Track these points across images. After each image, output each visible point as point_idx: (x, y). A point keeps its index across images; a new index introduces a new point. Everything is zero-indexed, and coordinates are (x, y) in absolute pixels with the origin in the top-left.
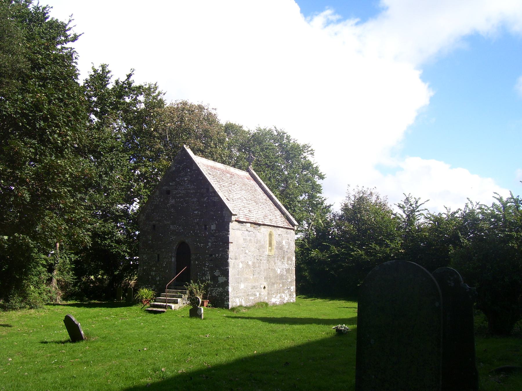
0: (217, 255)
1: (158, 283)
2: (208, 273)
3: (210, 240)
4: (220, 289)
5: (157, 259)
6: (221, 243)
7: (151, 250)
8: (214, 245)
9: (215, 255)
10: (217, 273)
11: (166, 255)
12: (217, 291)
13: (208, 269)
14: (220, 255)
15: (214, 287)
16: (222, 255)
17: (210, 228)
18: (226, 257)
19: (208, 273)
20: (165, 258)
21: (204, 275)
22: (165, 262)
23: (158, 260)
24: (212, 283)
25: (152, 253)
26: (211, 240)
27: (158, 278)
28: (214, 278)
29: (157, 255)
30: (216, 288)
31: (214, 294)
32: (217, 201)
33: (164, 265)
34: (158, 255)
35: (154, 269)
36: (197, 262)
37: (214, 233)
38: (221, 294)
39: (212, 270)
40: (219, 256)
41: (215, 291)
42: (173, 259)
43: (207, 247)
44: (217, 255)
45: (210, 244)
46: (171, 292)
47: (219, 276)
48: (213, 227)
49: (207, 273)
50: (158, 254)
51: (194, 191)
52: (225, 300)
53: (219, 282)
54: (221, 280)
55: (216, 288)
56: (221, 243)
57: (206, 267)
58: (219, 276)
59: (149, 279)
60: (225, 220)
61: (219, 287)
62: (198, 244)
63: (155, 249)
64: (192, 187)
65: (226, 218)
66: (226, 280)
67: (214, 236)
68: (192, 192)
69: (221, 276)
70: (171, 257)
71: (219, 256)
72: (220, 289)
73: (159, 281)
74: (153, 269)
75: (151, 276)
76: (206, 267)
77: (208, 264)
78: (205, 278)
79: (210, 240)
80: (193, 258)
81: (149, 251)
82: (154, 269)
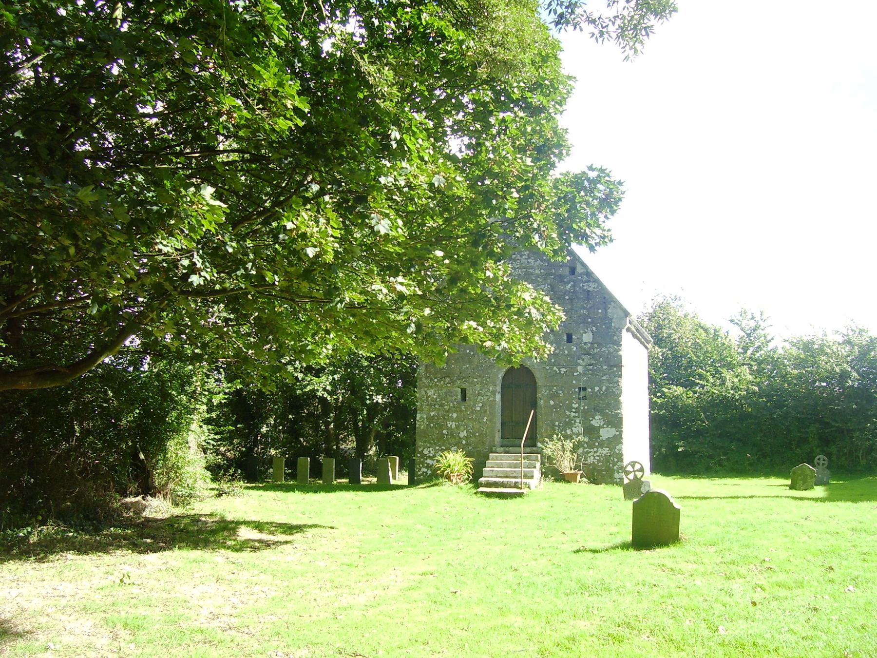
0: (597, 389)
1: (464, 442)
2: (578, 421)
3: (580, 361)
4: (605, 451)
5: (459, 396)
6: (605, 367)
7: (447, 380)
8: (590, 370)
9: (593, 389)
10: (596, 422)
11: (481, 390)
12: (598, 454)
13: (577, 415)
14: (604, 388)
15: (591, 446)
16: (608, 388)
17: (580, 339)
18: (617, 392)
19: (578, 421)
20: (479, 394)
21: (569, 424)
22: (479, 402)
23: (464, 398)
24: (586, 440)
25: (449, 385)
26: (583, 361)
27: (463, 434)
28: (591, 431)
29: (460, 390)
30: (595, 449)
31: (590, 460)
32: (595, 290)
33: (478, 409)
34: (463, 391)
35: (455, 415)
36: (552, 403)
37: (590, 348)
38: (607, 459)
39: (586, 416)
40: (601, 390)
41: (592, 454)
42: (498, 397)
43: (575, 374)
44: (597, 389)
45: (580, 369)
46: (499, 458)
47: (601, 427)
48: (587, 337)
49: (575, 422)
50: (462, 389)
51: (542, 271)
52: (614, 470)
53: (601, 438)
54: (606, 433)
55: (595, 449)
56: (605, 367)
57: (574, 410)
58: (601, 427)
59: (444, 434)
60: (613, 325)
61: (601, 445)
62: (555, 368)
63: (455, 378)
64: (537, 264)
65: (614, 320)
66: (618, 433)
67: (589, 354)
68: (537, 272)
69: (605, 426)
70: (494, 393)
71: (601, 390)
72: (605, 451)
73: (467, 438)
74: (452, 416)
75: (448, 429)
76: (574, 410)
77: (577, 405)
78: (572, 431)
79: (580, 361)
80: (543, 395)
81: (442, 382)
82: (455, 415)
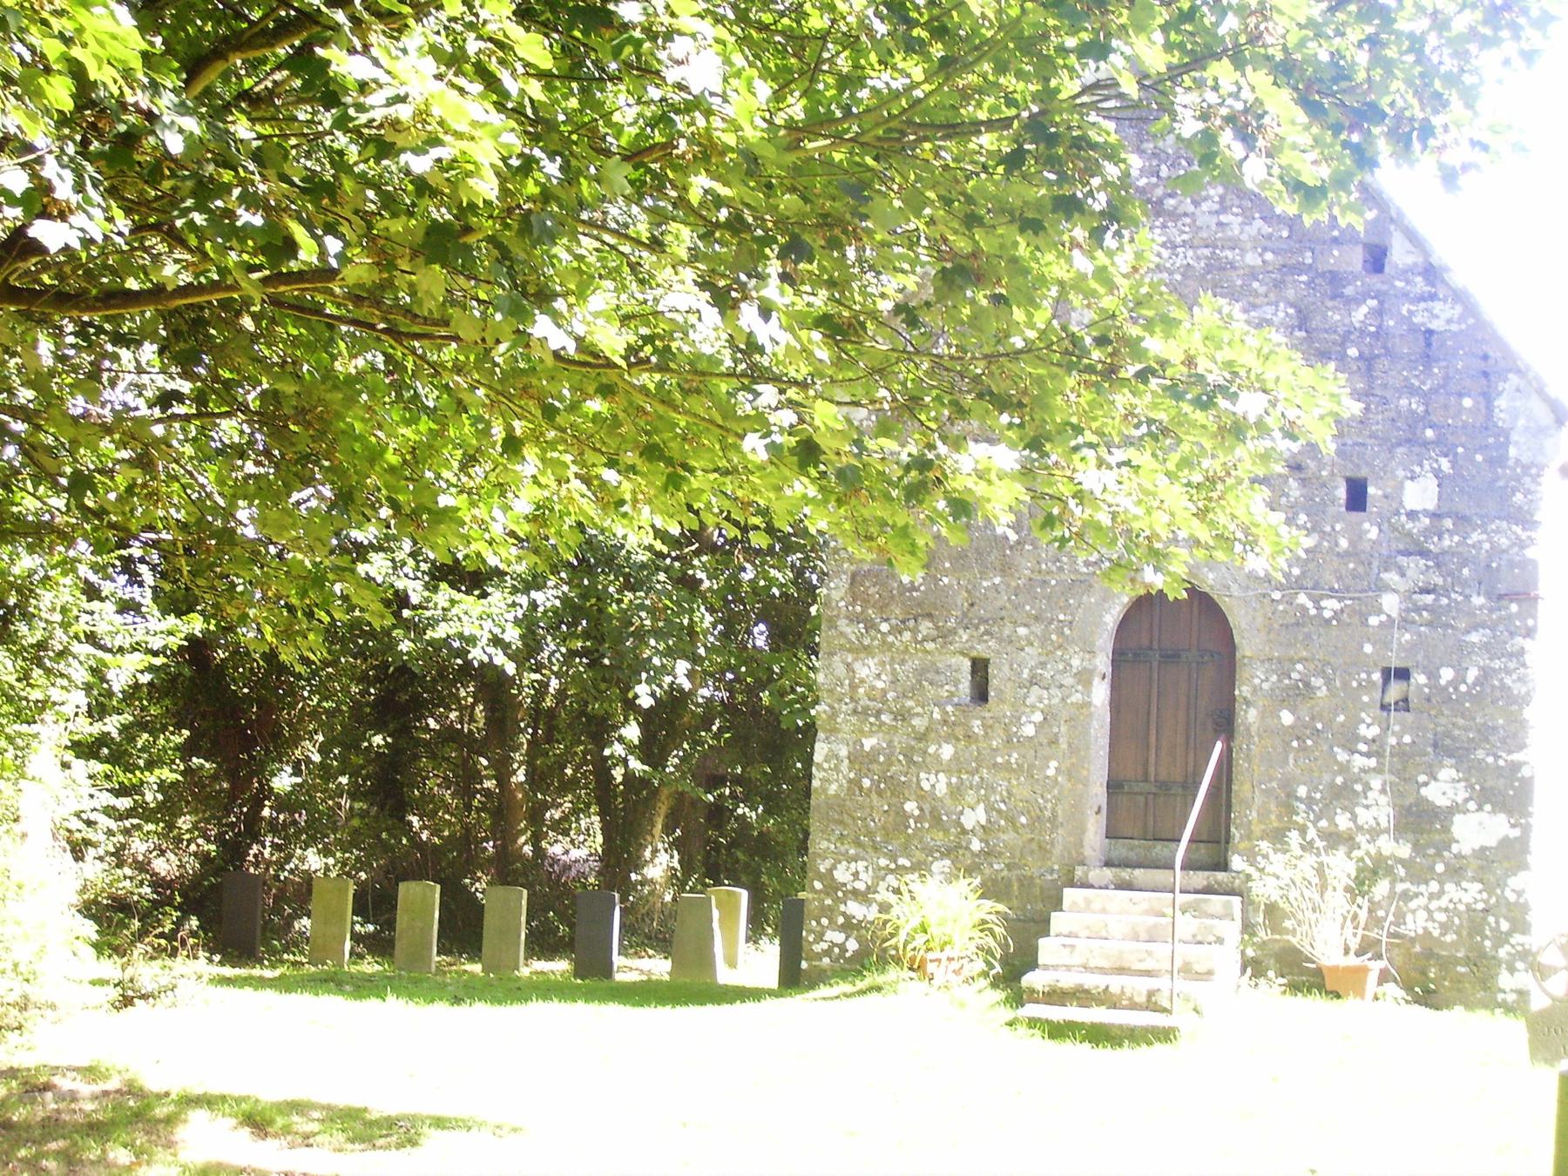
1: (976, 845)
2: (1376, 783)
3: (1391, 577)
4: (1470, 893)
5: (965, 686)
6: (1478, 600)
7: (926, 627)
8: (1426, 608)
9: (1433, 675)
10: (1442, 789)
11: (1043, 665)
12: (1444, 902)
13: (1373, 762)
14: (1472, 674)
15: (1419, 874)
16: (1486, 674)
17: (1394, 497)
18: (1518, 689)
19: (1376, 783)
20: (1034, 681)
21: (1345, 794)
23: (981, 694)
24: (1405, 851)
25: (930, 646)
26: (1403, 575)
27: (974, 817)
29: (967, 664)
31: (1416, 924)
32: (1454, 327)
33: (1029, 730)
34: (980, 668)
35: (947, 751)
36: (1287, 718)
37: (1427, 533)
38: (1475, 922)
41: (1422, 901)
42: (1100, 693)
44: (1447, 674)
45: (1391, 603)
47: (1455, 809)
48: (1420, 494)
49: (1367, 787)
51: (1269, 256)
53: (1455, 848)
55: (1434, 886)
59: (906, 816)
60: (1512, 452)
61: (1456, 872)
62: (1302, 599)
63: (952, 623)
64: (1252, 230)
65: (1514, 437)
66: (1515, 833)
67: (1424, 553)
68: (1252, 259)
69: (1472, 805)
70: (1085, 677)
71: (1460, 678)
72: (1470, 893)
74: (937, 756)
75: (921, 796)
76: (1363, 747)
78: (1354, 818)
79: (1391, 577)
80: (1255, 690)
81: (907, 635)
82: (947, 751)
